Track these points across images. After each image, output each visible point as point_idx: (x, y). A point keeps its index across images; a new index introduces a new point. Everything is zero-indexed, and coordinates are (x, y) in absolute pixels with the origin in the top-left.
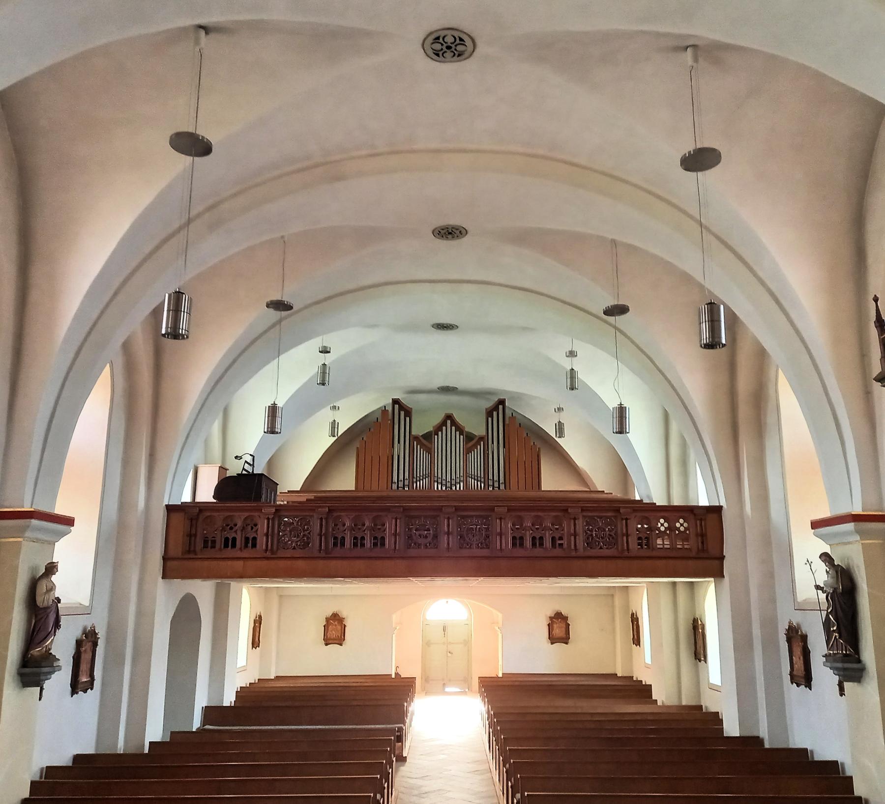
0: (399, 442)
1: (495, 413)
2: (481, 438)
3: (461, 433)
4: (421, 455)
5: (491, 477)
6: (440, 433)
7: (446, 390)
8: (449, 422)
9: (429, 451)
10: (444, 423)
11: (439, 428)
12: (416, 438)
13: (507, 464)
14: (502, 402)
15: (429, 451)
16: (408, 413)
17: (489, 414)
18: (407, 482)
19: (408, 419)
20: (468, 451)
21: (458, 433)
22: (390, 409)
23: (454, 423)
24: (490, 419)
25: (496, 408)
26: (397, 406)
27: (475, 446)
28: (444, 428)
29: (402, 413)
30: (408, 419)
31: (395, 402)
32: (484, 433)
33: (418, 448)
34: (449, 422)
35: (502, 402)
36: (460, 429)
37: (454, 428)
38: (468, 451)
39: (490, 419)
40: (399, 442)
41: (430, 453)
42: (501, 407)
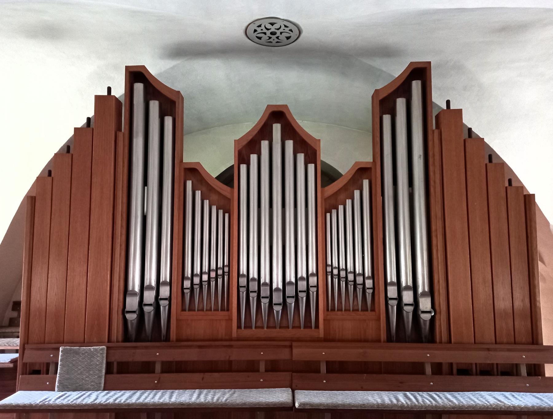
0: (145, 183)
1: (401, 103)
2: (362, 171)
3: (312, 156)
4: (205, 219)
5: (391, 276)
6: (254, 158)
7: (272, 39)
8: (277, 128)
9: (227, 206)
10: (264, 132)
11: (247, 149)
12: (194, 172)
13: (438, 242)
14: (420, 72)
15: (227, 206)
16: (171, 104)
17: (385, 104)
18: (165, 291)
19: (168, 121)
20: (328, 205)
21: (301, 157)
22: (119, 91)
23: (291, 131)
24: (387, 119)
25: (403, 88)
26: (139, 87)
27: (347, 191)
28: (265, 144)
29: (154, 106)
30: (168, 121)
31: (136, 75)
32: (366, 157)
33: (194, 196)
34: (277, 128)
35: (420, 72)
36: (307, 148)
37: (290, 144)
38: (328, 205)
39: (387, 119)
40: (145, 183)
41: (227, 210)
42: (416, 86)
